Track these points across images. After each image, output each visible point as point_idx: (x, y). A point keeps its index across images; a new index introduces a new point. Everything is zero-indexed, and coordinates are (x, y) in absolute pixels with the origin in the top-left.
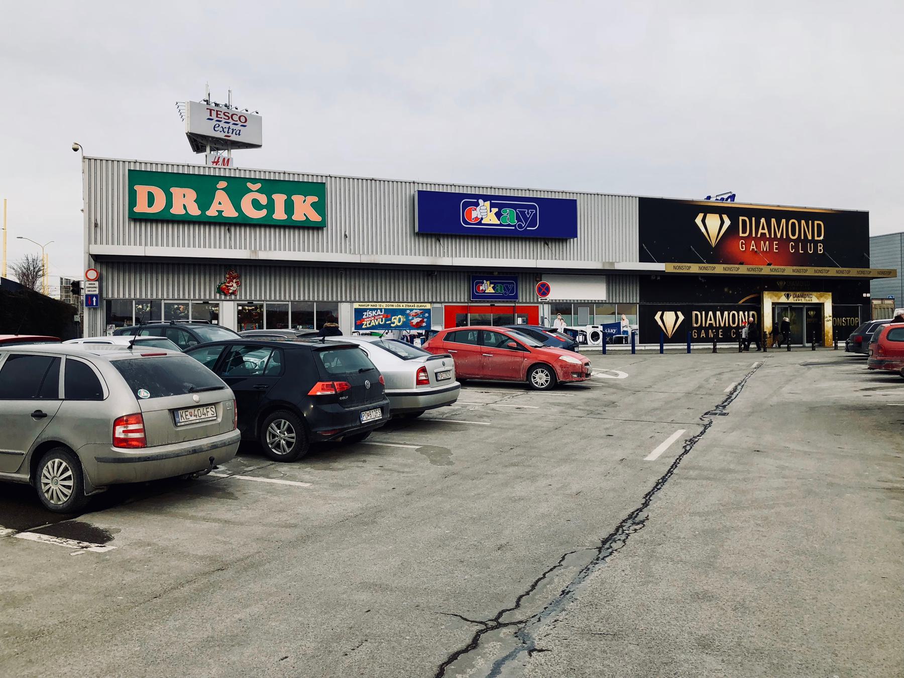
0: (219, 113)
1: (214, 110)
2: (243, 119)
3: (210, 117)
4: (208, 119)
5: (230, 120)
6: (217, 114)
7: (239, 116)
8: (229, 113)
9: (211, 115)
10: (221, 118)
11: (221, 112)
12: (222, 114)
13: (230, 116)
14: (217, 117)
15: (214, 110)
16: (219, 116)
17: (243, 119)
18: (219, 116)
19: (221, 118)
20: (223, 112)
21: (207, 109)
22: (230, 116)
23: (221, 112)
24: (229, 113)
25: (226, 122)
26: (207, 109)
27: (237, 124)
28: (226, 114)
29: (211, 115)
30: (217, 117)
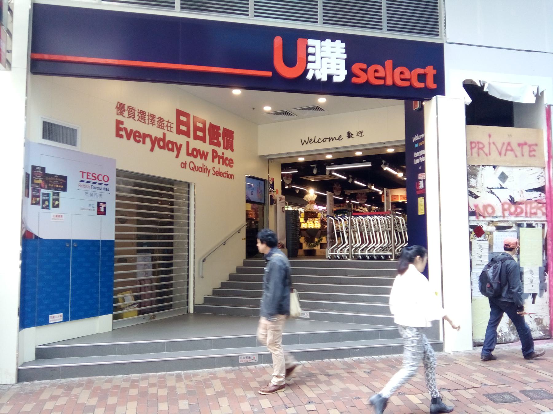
0: (89, 174)
1: (85, 172)
2: (106, 179)
5: (97, 181)
6: (88, 176)
8: (96, 174)
9: (83, 178)
10: (90, 179)
11: (90, 173)
12: (90, 175)
13: (96, 176)
14: (88, 178)
15: (85, 172)
16: (89, 177)
17: (106, 179)
18: (89, 177)
19: (90, 179)
20: (92, 173)
21: (81, 172)
23: (90, 173)
24: (96, 174)
26: (81, 172)
28: (94, 175)
29: (83, 178)
30: (88, 178)
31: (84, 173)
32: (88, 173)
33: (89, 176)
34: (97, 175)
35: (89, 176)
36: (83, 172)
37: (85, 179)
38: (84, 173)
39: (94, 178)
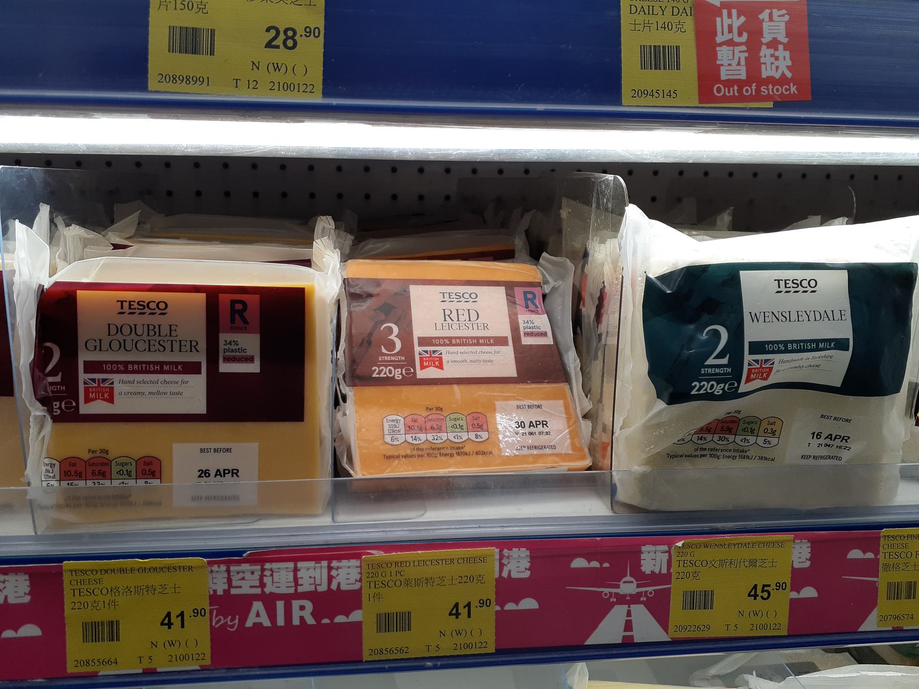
0: (787, 282)
1: (782, 280)
3: (779, 290)
4: (778, 292)
5: (800, 288)
6: (786, 284)
7: (808, 280)
8: (797, 280)
9: (779, 287)
10: (790, 287)
11: (789, 280)
13: (799, 283)
14: (786, 287)
15: (782, 280)
16: (788, 286)
17: (813, 283)
19: (790, 287)
20: (791, 281)
21: (775, 280)
22: (799, 283)
23: (789, 280)
24: (797, 280)
25: (795, 292)
26: (775, 280)
27: (806, 292)
28: (795, 281)
29: (779, 287)
31: (780, 281)
32: (785, 280)
33: (788, 284)
34: (799, 281)
35: (788, 284)
36: (779, 281)
37: (782, 288)
38: (780, 281)
39: (796, 286)
